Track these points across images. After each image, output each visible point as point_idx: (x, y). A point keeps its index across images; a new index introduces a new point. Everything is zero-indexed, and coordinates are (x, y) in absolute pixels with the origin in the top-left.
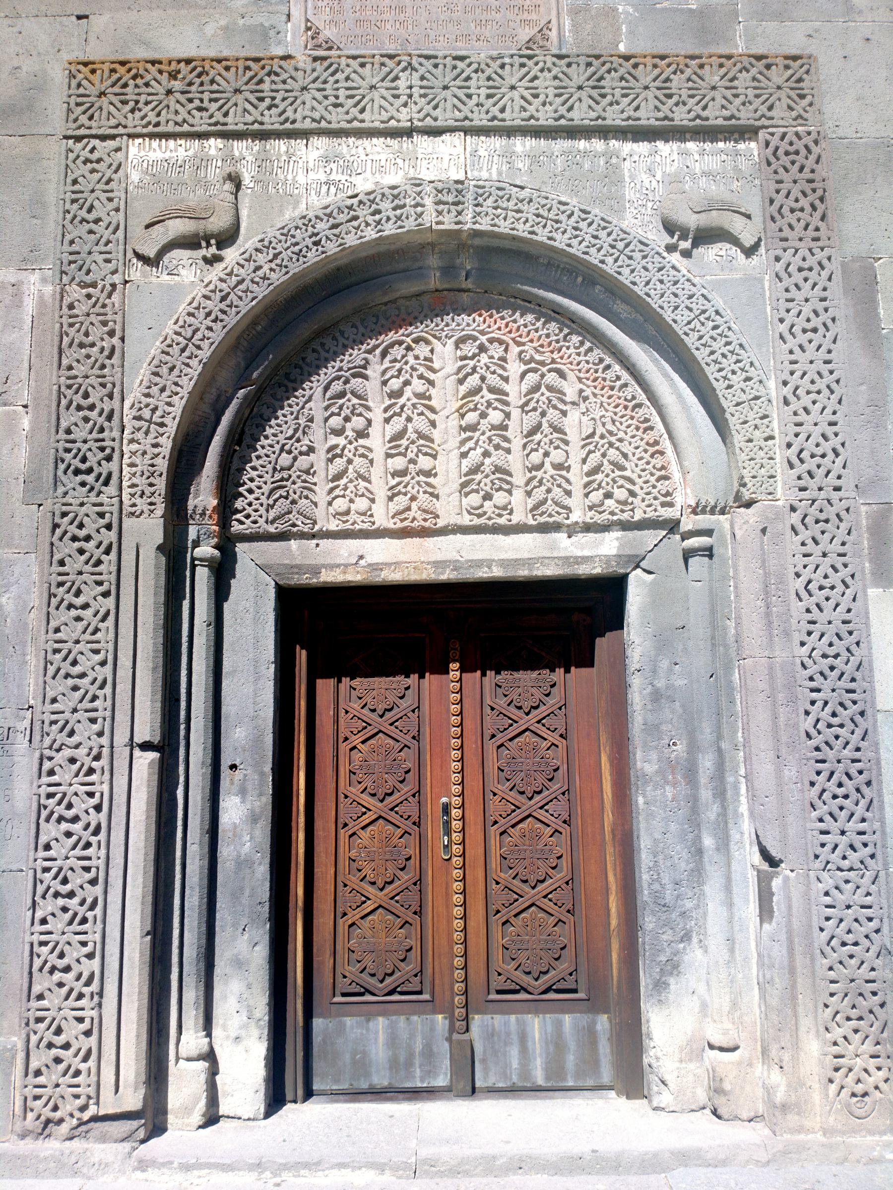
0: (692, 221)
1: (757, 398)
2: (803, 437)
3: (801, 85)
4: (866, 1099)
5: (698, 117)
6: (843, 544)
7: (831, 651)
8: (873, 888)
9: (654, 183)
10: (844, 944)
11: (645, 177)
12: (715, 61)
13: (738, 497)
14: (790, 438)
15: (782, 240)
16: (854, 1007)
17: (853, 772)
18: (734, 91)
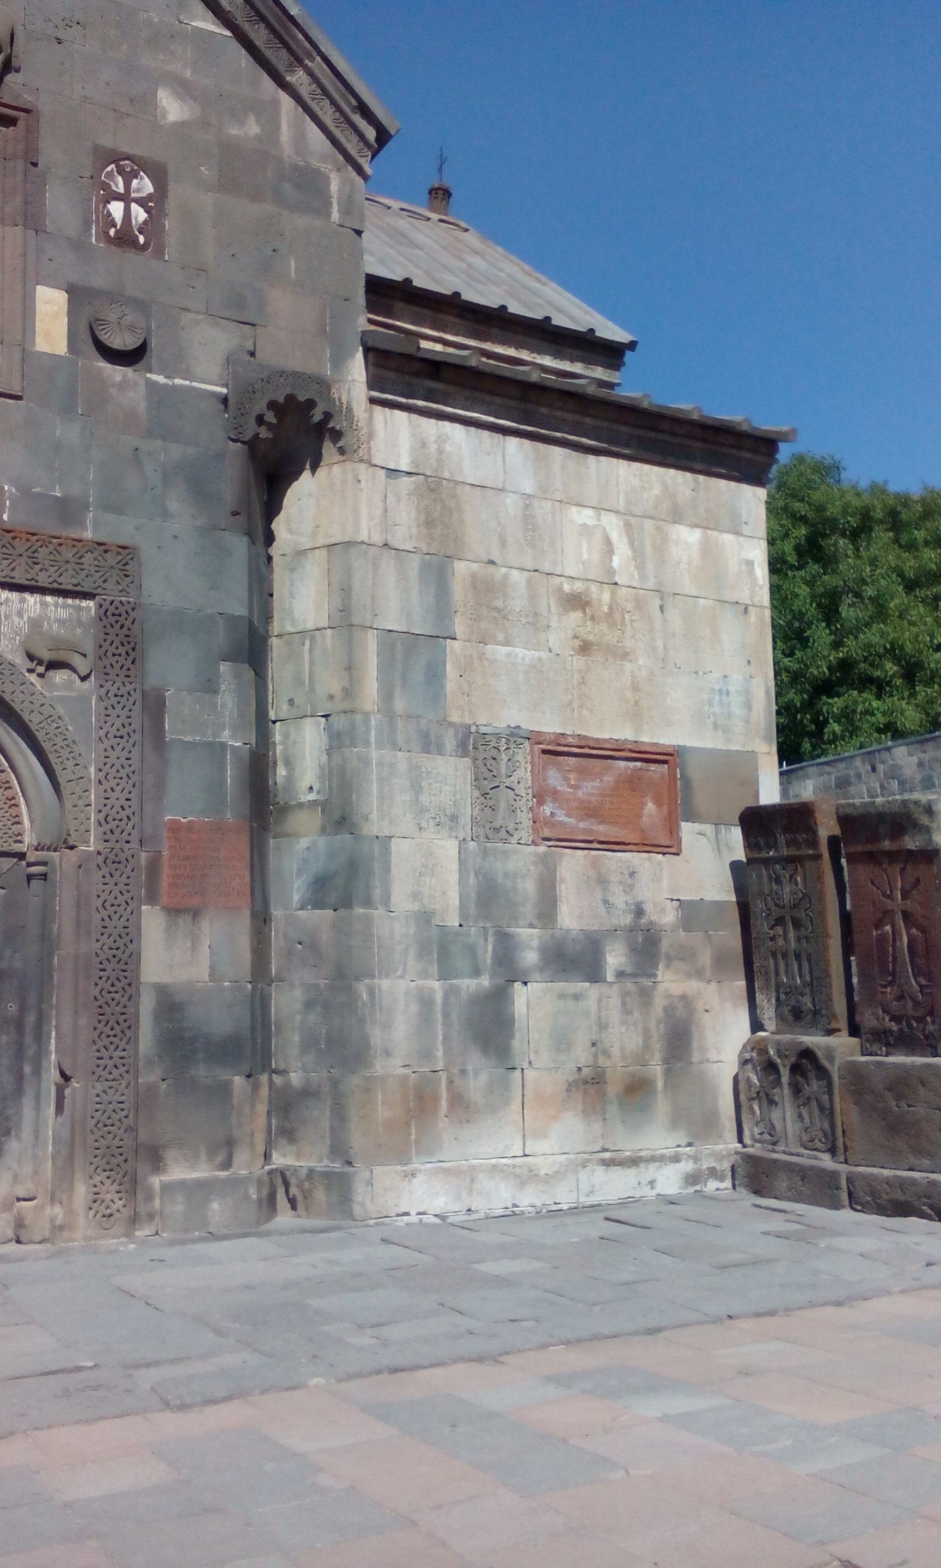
0: (46, 655)
1: (82, 778)
2: (108, 807)
3: (126, 567)
4: (112, 1218)
5: (55, 581)
6: (128, 878)
7: (115, 946)
8: (126, 1091)
9: (22, 623)
10: (106, 1126)
11: (16, 619)
12: (70, 542)
13: (65, 841)
14: (101, 807)
15: (106, 674)
16: (108, 1163)
17: (121, 1021)
18: (81, 566)
